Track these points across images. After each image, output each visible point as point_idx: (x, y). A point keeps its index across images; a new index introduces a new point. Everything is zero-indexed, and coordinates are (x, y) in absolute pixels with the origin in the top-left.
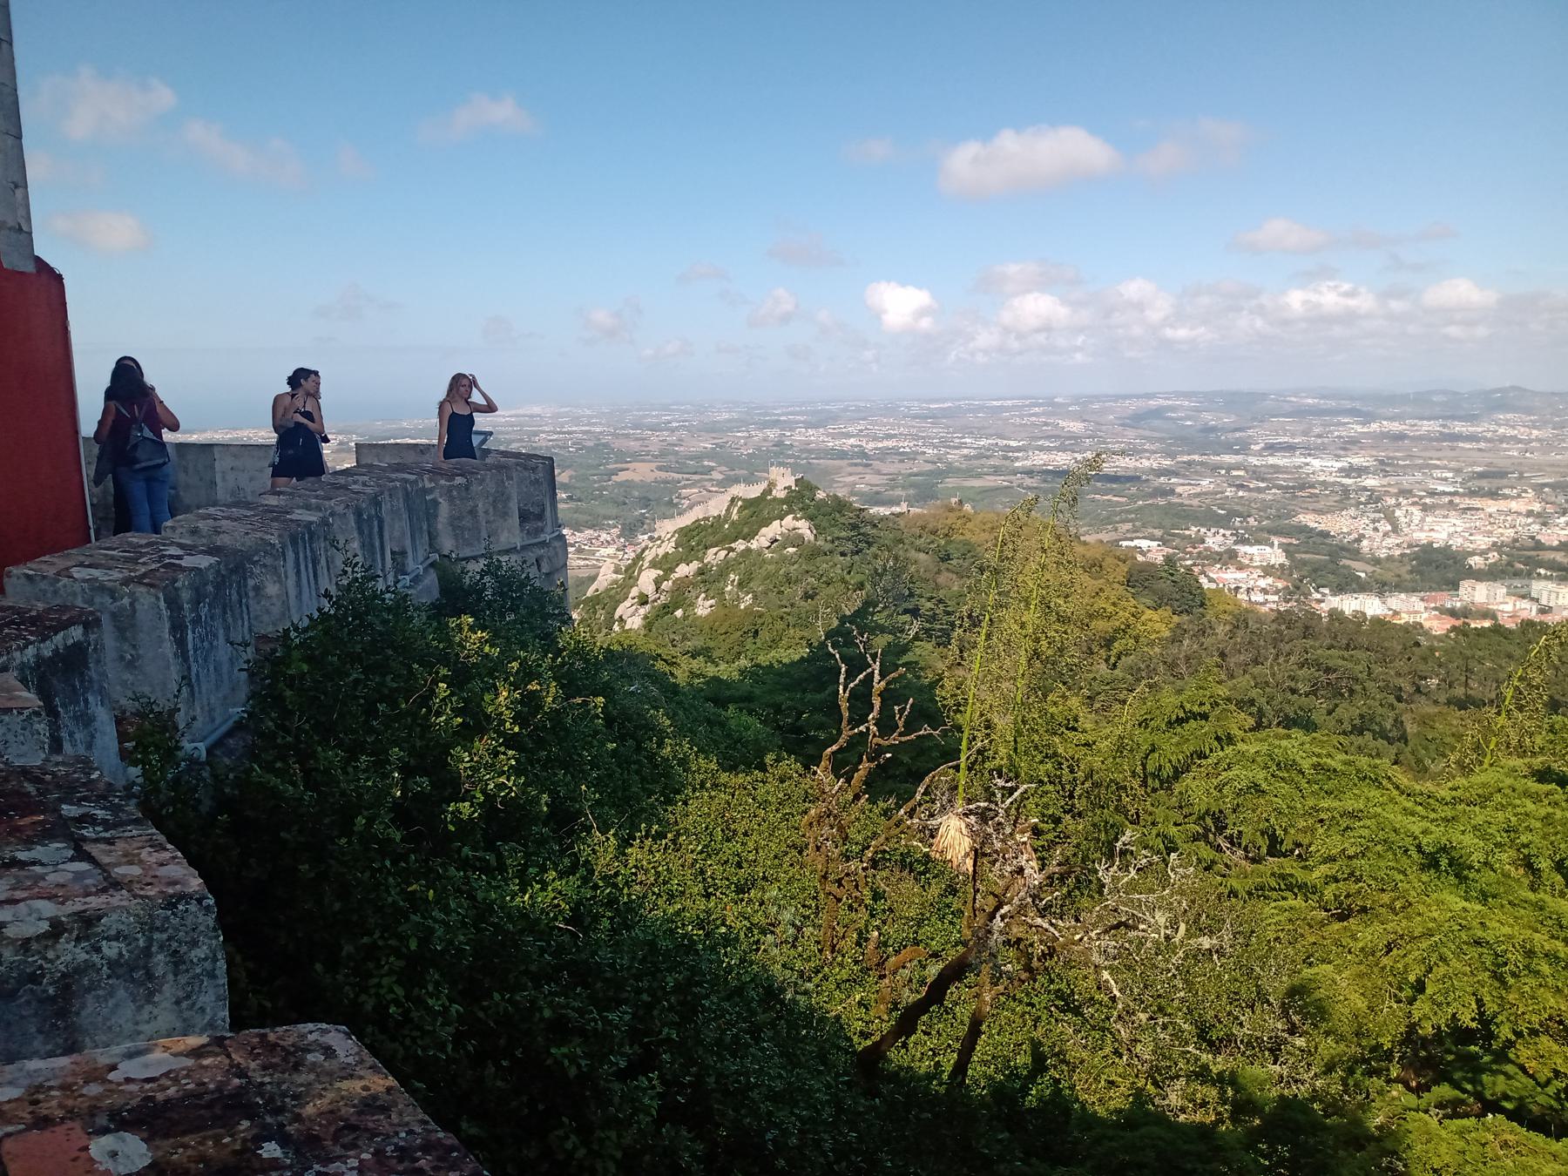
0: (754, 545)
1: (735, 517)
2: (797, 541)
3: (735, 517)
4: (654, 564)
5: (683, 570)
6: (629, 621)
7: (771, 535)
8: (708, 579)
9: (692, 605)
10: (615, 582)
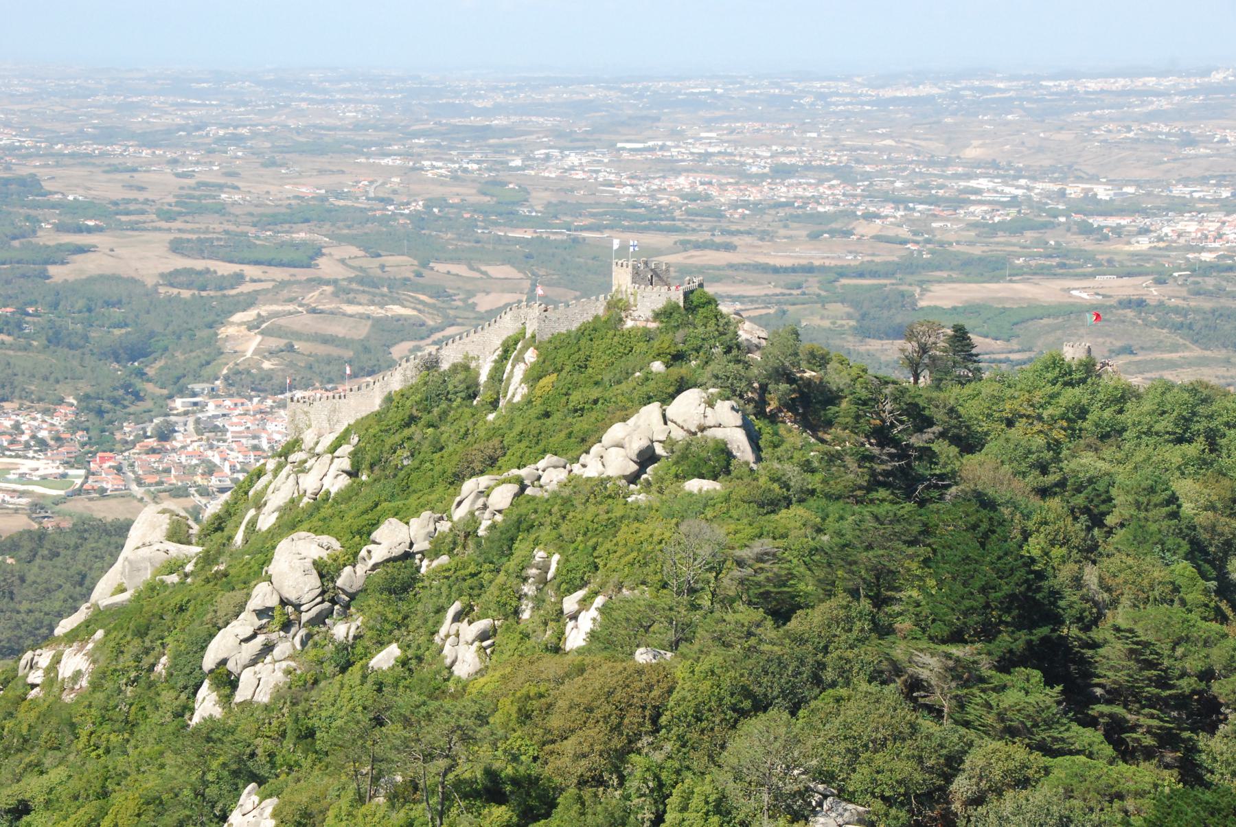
0: (591, 467)
1: (517, 390)
2: (719, 462)
3: (517, 390)
5: (390, 537)
8: (483, 567)
10: (174, 566)
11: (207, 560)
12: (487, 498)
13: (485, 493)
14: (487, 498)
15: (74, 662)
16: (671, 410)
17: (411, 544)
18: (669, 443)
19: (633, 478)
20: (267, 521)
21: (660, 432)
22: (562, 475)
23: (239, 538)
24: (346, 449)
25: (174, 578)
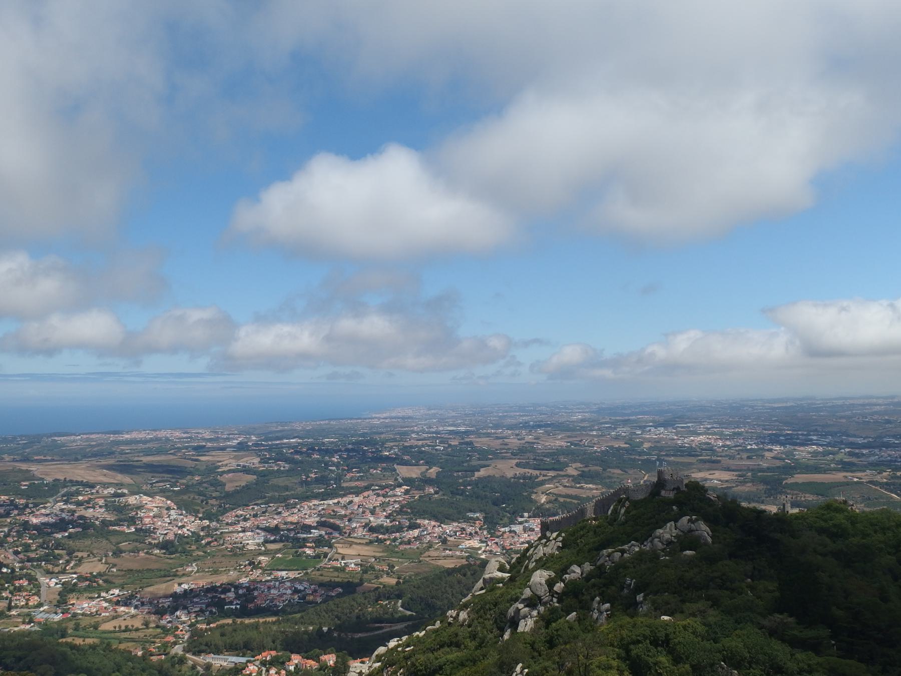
0: (647, 547)
3: (622, 518)
4: (542, 564)
6: (522, 623)
7: (667, 536)
9: (590, 609)
11: (511, 579)
12: (610, 556)
13: (609, 556)
14: (610, 556)
15: (463, 615)
16: (679, 524)
17: (582, 574)
18: (677, 537)
19: (663, 550)
20: (531, 566)
21: (675, 532)
22: (637, 549)
23: (522, 571)
24: (560, 539)
25: (501, 585)
